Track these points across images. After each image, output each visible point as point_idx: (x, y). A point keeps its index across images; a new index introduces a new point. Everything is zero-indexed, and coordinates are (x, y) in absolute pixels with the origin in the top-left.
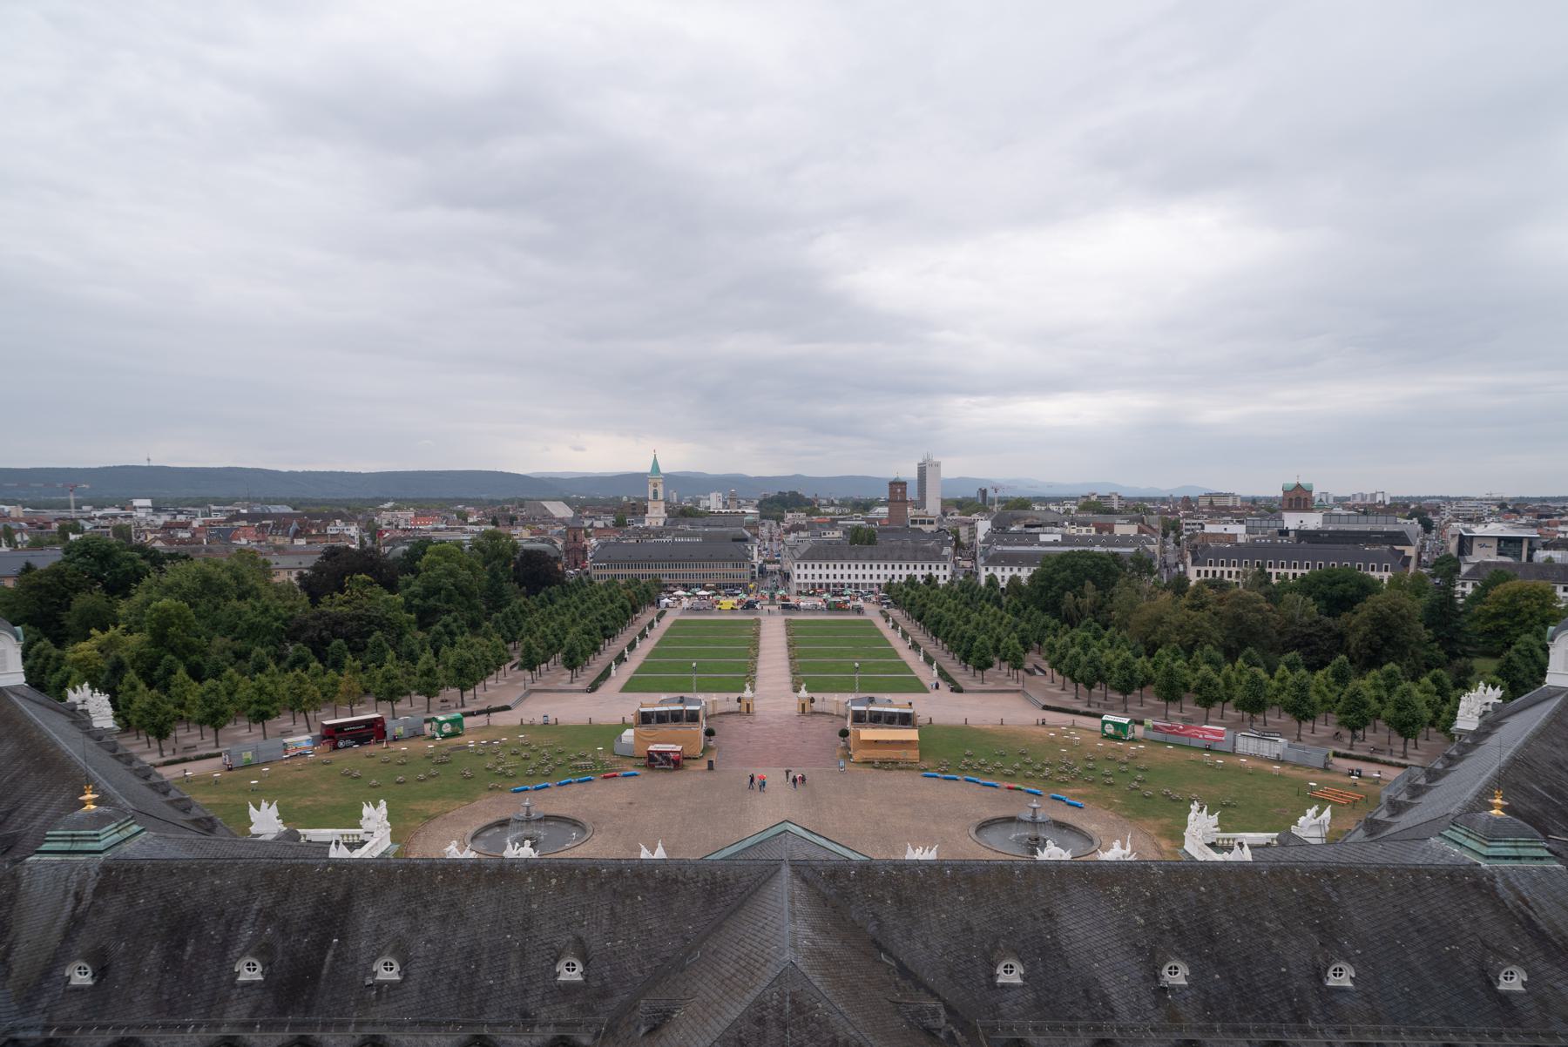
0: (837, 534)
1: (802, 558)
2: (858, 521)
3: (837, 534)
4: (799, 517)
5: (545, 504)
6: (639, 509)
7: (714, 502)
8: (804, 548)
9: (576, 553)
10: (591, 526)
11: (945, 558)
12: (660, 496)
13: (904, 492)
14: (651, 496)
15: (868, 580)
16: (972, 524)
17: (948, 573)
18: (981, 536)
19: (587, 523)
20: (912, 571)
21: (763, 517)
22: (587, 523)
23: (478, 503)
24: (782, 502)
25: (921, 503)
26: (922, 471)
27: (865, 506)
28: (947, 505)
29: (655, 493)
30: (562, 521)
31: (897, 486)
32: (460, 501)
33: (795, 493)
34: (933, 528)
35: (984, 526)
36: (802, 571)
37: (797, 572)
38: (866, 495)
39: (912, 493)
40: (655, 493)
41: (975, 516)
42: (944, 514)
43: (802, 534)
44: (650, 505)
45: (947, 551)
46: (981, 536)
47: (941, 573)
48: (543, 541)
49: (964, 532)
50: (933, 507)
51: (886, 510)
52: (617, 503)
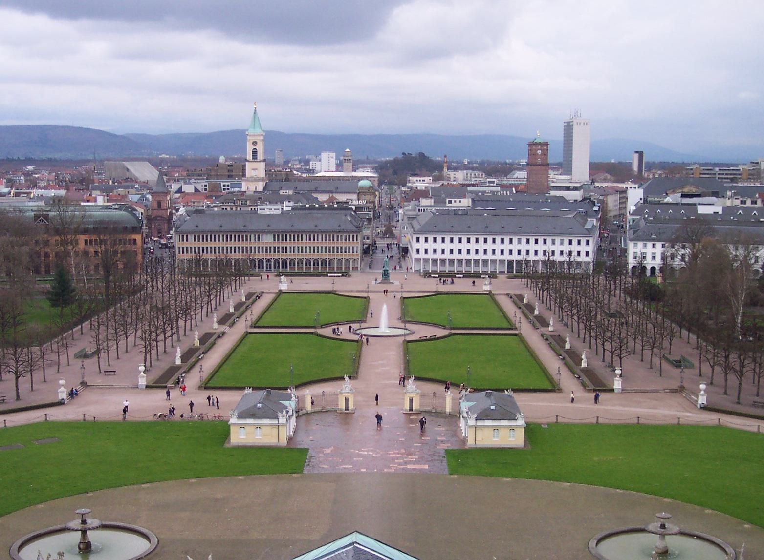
0: (466, 202)
1: (421, 231)
2: (491, 187)
3: (466, 202)
4: (421, 183)
5: (128, 165)
6: (236, 171)
7: (326, 166)
8: (424, 218)
9: (160, 221)
10: (180, 191)
11: (589, 232)
12: (260, 156)
13: (545, 154)
14: (249, 156)
15: (498, 257)
16: (624, 192)
17: (591, 248)
18: (631, 207)
19: (175, 187)
20: (549, 247)
21: (381, 183)
22: (175, 187)
23: (50, 163)
24: (403, 165)
25: (566, 167)
26: (568, 129)
27: (504, 170)
28: (596, 168)
29: (255, 153)
30: (145, 185)
31: (537, 148)
32: (29, 161)
33: (422, 155)
34: (577, 195)
35: (635, 195)
36: (422, 245)
37: (416, 245)
38: (495, 157)
39: (555, 155)
40: (255, 153)
41: (629, 184)
42: (593, 182)
43: (424, 202)
44: (248, 166)
45: (592, 222)
46: (631, 207)
47: (583, 248)
48: (120, 209)
49: (612, 202)
50: (581, 172)
51: (523, 174)
52: (209, 162)
